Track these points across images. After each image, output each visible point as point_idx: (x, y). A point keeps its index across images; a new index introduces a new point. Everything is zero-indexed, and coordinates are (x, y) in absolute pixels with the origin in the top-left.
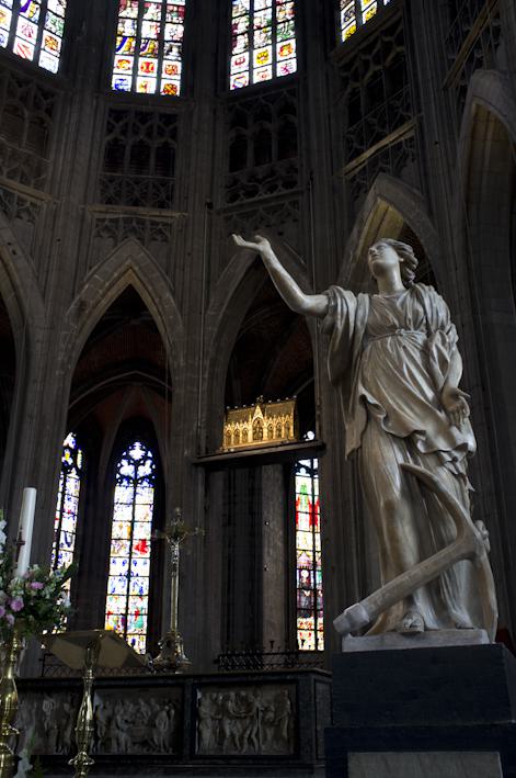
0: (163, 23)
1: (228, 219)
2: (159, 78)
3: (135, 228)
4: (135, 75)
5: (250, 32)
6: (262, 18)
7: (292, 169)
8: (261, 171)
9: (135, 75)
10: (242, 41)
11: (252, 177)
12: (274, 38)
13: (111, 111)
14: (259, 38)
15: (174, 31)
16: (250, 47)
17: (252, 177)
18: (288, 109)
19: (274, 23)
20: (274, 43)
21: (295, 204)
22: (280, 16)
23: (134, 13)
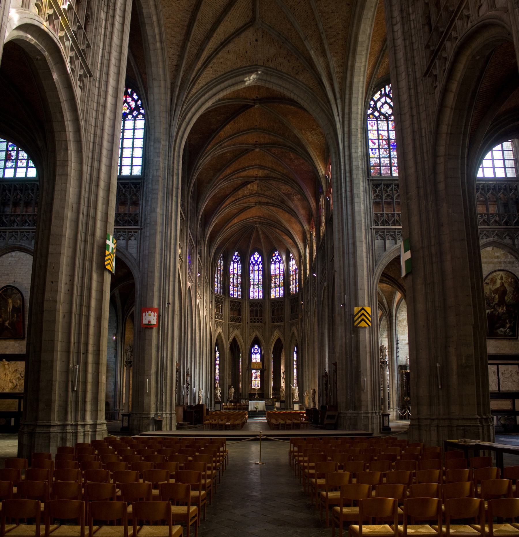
0: (238, 279)
1: (251, 327)
2: (238, 293)
3: (237, 327)
4: (234, 292)
5: (254, 284)
6: (256, 282)
7: (261, 319)
8: (256, 318)
9: (234, 292)
10: (252, 286)
11: (255, 319)
12: (258, 287)
13: (231, 301)
14: (256, 287)
15: (240, 280)
16: (254, 288)
17: (255, 319)
18: (261, 306)
19: (258, 284)
20: (258, 289)
21: (262, 327)
22: (259, 282)
23: (232, 277)
